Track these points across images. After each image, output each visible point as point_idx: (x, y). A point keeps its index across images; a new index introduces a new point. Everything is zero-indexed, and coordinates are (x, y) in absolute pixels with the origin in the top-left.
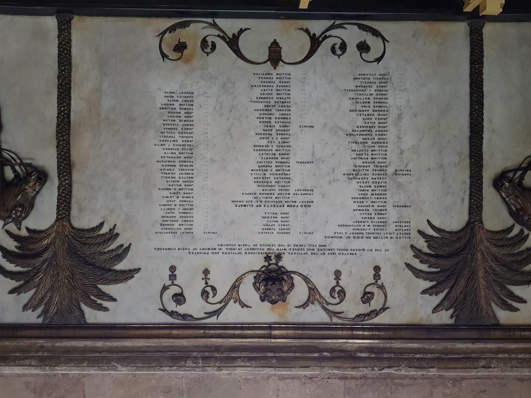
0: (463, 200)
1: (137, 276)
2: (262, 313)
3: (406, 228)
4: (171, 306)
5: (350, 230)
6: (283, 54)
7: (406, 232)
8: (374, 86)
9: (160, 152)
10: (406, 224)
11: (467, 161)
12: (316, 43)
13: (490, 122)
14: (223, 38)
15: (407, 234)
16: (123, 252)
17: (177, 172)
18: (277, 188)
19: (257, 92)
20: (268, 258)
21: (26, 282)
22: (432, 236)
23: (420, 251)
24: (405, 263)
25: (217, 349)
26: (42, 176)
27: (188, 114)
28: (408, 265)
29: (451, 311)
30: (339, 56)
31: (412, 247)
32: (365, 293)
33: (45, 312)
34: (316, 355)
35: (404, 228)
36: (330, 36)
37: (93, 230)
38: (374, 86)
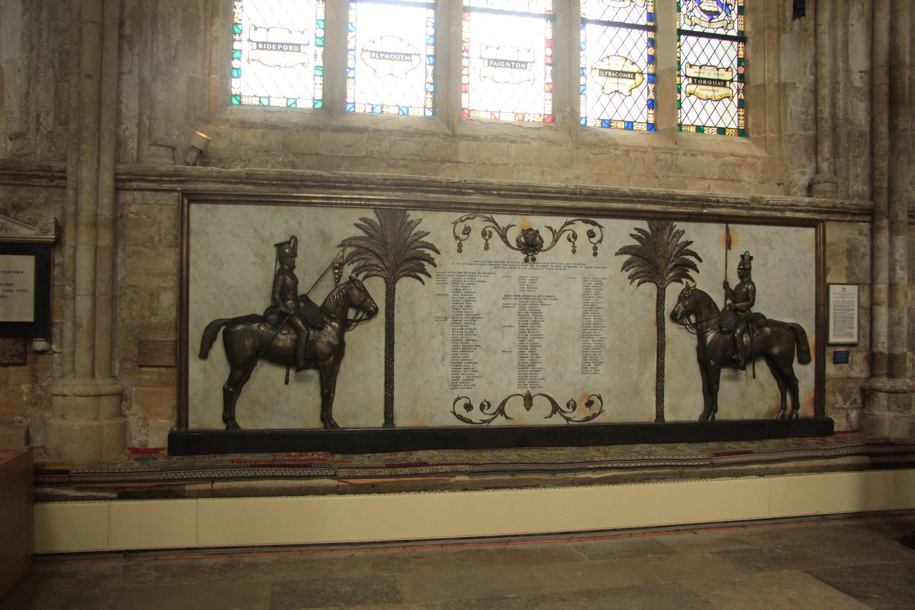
0: (399, 299)
2: (539, 223)
4: (596, 229)
5: (478, 278)
6: (523, 402)
9: (603, 333)
11: (396, 327)
12: (501, 411)
13: (379, 355)
14: (562, 411)
16: (625, 267)
17: (592, 320)
18: (527, 309)
19: (540, 375)
20: (534, 260)
21: (682, 248)
22: (421, 273)
25: (565, 199)
26: (674, 317)
27: (585, 359)
28: (438, 252)
29: (409, 219)
31: (435, 266)
32: (468, 234)
33: (672, 229)
34: (502, 192)
37: (644, 282)
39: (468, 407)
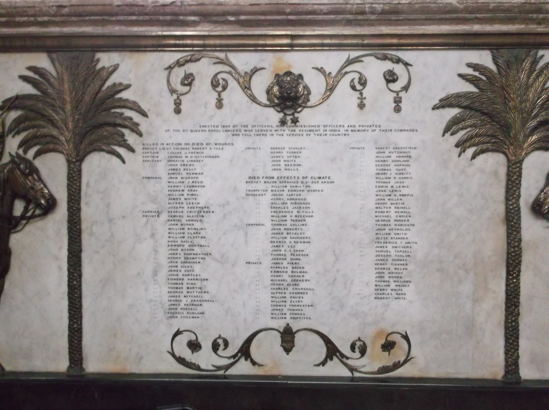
0: (88, 185)
1: (436, 101)
3: (147, 155)
4: (399, 69)
5: (207, 152)
6: (279, 340)
7: (147, 151)
8: (182, 305)
9: (411, 235)
10: (147, 159)
11: (84, 226)
12: (245, 351)
13: (60, 268)
14: (343, 356)
15: (146, 148)
16: (451, 127)
17: (393, 215)
18: (285, 197)
19: (307, 299)
20: (295, 121)
22: (120, 146)
23: (133, 130)
24: (147, 117)
26: (537, 209)
27: (380, 276)
28: (144, 114)
29: (99, 66)
30: (220, 337)
31: (140, 135)
32: (190, 84)
33: (535, 62)
34: (243, 18)
35: (149, 155)
36: (229, 358)
37: (483, 152)
38: (182, 305)
39: (194, 346)
